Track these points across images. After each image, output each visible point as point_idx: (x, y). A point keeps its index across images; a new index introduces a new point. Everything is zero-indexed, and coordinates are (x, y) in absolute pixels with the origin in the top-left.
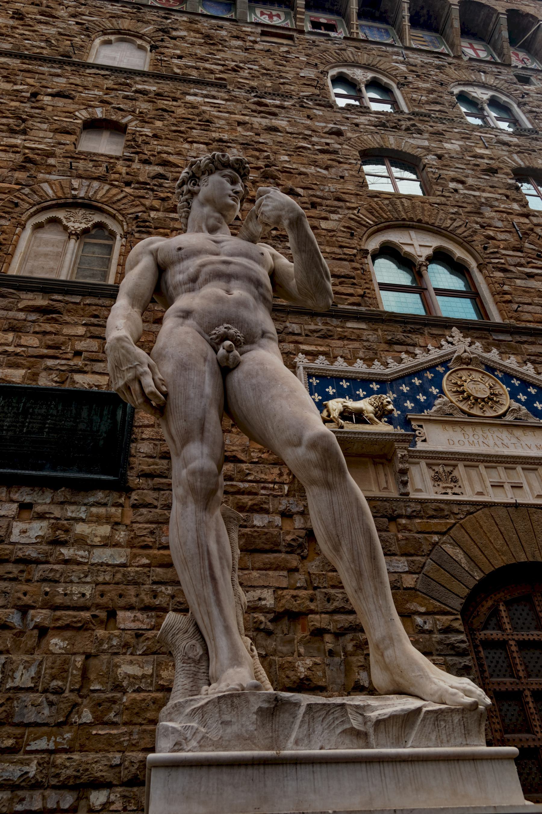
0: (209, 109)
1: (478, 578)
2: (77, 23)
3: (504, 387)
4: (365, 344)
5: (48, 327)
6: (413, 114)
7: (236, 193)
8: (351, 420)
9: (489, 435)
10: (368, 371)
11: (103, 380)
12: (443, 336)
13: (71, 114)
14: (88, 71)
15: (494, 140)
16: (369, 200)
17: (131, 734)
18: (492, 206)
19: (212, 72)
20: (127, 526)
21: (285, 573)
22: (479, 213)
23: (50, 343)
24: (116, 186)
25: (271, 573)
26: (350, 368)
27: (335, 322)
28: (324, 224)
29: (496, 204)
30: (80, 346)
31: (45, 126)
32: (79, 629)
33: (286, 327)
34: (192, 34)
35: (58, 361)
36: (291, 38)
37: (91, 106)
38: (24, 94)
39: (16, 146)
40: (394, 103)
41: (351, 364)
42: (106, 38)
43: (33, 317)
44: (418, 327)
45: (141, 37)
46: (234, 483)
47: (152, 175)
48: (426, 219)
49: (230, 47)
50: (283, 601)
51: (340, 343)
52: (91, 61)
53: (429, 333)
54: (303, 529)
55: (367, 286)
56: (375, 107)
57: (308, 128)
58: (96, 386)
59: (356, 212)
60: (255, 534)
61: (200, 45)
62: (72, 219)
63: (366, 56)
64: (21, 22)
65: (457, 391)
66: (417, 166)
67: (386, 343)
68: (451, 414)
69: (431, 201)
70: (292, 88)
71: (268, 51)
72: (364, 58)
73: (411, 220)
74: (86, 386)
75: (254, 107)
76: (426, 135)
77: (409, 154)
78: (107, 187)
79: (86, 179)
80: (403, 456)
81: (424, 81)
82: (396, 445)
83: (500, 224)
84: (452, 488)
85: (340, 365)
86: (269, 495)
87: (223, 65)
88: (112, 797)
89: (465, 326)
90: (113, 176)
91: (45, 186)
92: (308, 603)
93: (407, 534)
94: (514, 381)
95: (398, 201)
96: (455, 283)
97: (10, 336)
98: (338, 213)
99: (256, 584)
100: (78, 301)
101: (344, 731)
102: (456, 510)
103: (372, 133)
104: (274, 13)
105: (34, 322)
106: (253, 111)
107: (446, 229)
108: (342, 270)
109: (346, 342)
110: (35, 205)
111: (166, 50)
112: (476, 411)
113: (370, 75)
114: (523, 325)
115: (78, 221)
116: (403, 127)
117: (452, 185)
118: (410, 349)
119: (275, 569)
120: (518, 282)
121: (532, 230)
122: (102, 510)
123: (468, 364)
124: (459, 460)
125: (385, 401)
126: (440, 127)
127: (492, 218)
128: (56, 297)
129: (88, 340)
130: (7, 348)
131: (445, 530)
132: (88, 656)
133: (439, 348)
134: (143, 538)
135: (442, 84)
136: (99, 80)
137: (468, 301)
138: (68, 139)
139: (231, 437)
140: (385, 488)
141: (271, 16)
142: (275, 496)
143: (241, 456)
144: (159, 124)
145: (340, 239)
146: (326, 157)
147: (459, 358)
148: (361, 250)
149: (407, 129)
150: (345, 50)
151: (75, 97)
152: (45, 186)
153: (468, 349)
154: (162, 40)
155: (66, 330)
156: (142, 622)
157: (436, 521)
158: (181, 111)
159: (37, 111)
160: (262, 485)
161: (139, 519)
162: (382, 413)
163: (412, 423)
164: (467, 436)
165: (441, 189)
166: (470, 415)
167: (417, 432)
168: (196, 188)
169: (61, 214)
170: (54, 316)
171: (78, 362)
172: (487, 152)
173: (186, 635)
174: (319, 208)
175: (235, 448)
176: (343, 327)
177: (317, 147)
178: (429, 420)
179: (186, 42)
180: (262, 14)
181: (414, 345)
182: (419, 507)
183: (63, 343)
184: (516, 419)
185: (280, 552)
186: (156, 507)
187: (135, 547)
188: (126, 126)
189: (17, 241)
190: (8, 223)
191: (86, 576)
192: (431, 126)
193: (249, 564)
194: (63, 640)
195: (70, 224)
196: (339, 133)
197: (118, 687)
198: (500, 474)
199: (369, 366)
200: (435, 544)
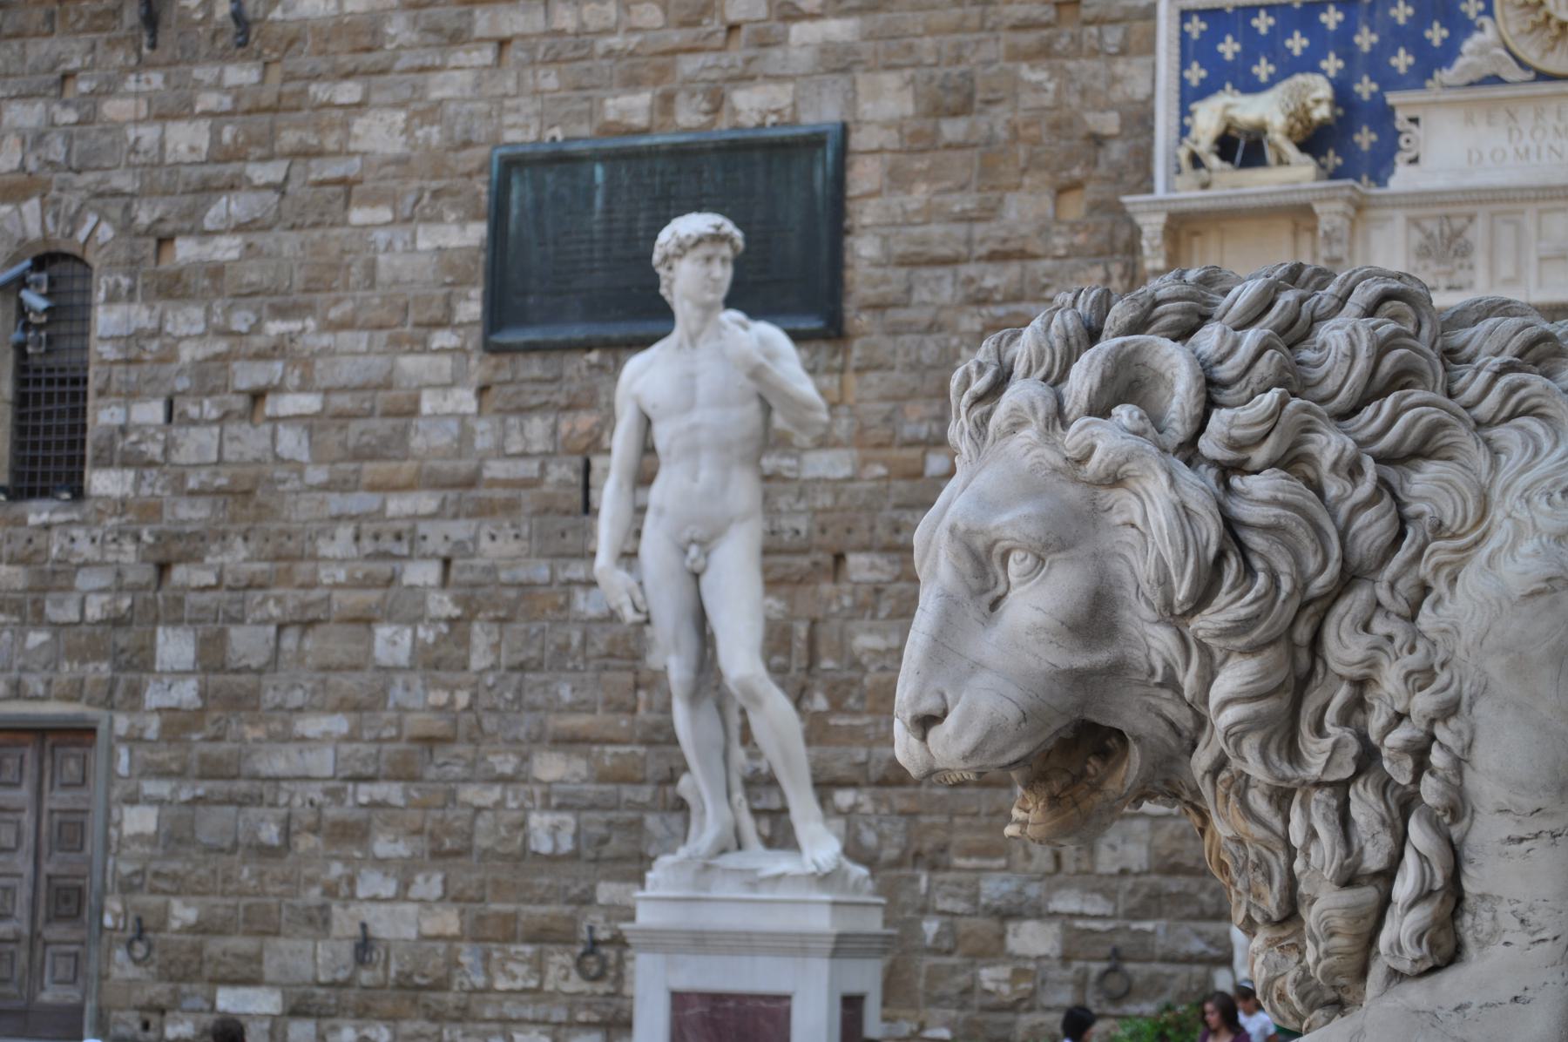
11: (781, 96)
17: (877, 724)
20: (851, 407)
32: (800, 582)
58: (776, 112)
68: (1495, 80)
82: (1317, 208)
88: (861, 799)
124: (1480, 202)
125: (1310, 104)
132: (814, 623)
143: (1034, 246)
156: (882, 571)
164: (1516, 134)
168: (671, 275)
171: (736, 55)
175: (1024, 230)
186: (892, 368)
191: (798, 500)
194: (780, 598)
197: (856, 664)
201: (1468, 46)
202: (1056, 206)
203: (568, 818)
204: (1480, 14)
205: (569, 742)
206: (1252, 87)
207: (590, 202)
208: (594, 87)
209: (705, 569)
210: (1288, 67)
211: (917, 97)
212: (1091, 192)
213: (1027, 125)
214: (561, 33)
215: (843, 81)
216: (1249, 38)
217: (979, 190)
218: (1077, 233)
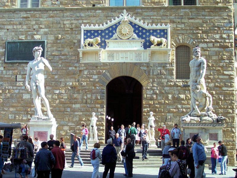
9: (124, 44)
12: (121, 12)
25: (71, 79)
27: (93, 11)
30: (34, 27)
46: (66, 60)
53: (118, 12)
68: (116, 39)
97: (20, 26)
100: (33, 13)
129: (36, 25)
143: (68, 54)
166: (121, 39)
176: (95, 13)
181: (113, 17)
184: (133, 39)
201: (114, 35)
203: (13, 115)
205: (12, 107)
206: (91, 38)
207: (17, 47)
210: (95, 37)
211: (55, 38)
215: (46, 35)
216: (91, 33)
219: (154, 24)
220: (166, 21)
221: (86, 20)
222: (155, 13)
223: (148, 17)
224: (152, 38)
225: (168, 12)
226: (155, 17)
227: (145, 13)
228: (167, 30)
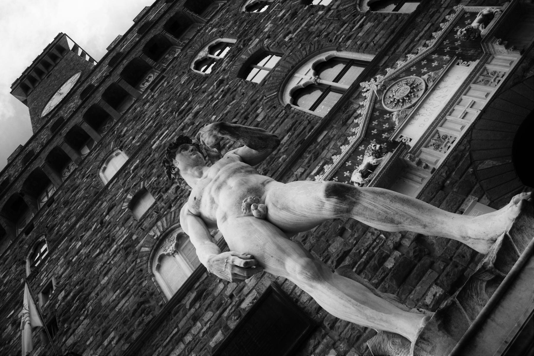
0: (165, 140)
1: (510, 161)
2: (87, 178)
3: (411, 76)
4: (335, 138)
5: (208, 302)
6: (239, 38)
7: (192, 150)
8: (370, 173)
10: (350, 146)
12: (361, 92)
13: (121, 211)
14: (109, 188)
15: (280, 5)
16: (264, 87)
18: (312, 25)
19: (151, 127)
20: (339, 340)
21: (430, 270)
22: (311, 33)
23: (216, 306)
24: (167, 214)
25: (424, 279)
26: (342, 155)
27: (312, 147)
28: (259, 119)
29: (312, 22)
31: (118, 228)
33: (296, 175)
34: (128, 125)
35: (228, 310)
36: (163, 77)
37: (124, 199)
38: (98, 227)
39: (116, 249)
40: (228, 44)
41: (340, 153)
42: (102, 168)
43: (197, 305)
44: (346, 103)
45: (113, 152)
46: (359, 263)
47: (174, 191)
48: (294, 63)
49: (147, 110)
50: (445, 283)
51: (325, 152)
52: (106, 183)
54: (412, 242)
55: (306, 116)
56: (222, 56)
57: (208, 96)
58: (254, 299)
59: (265, 98)
60: (395, 271)
61: (135, 124)
62: (167, 248)
63: (196, 45)
64: (70, 204)
65: (396, 104)
66: (266, 51)
67: (343, 126)
69: (287, 55)
70: (185, 91)
71: (161, 92)
72: (197, 46)
73: (289, 71)
74: (250, 305)
75: (180, 117)
76: (254, 38)
77: (256, 52)
78: (164, 219)
79: (153, 226)
80: (410, 158)
81: (228, 23)
83: (324, 26)
84: (448, 142)
85: (336, 159)
86: (379, 249)
87: (151, 119)
89: (364, 77)
90: (161, 212)
91: (144, 249)
92: (456, 270)
93: (457, 185)
94: (412, 69)
95: (275, 72)
96: (339, 68)
97: (199, 324)
98: (259, 108)
99: (424, 292)
101: (487, 287)
102: (462, 148)
103: (233, 65)
104: (147, 78)
105: (200, 307)
106: (181, 119)
107: (306, 56)
108: (288, 125)
109: (327, 148)
110: (147, 262)
111: (126, 143)
112: (414, 101)
113: (207, 49)
114: (385, 45)
115: (170, 246)
116: (242, 47)
117: (287, 39)
118: (355, 115)
119: (424, 274)
120: (360, 34)
121: (338, 11)
122: (321, 347)
123: (385, 89)
124: (435, 127)
125: (373, 148)
126: (255, 28)
127: (318, 28)
128: (196, 286)
130: (203, 331)
131: (469, 162)
133: (366, 99)
134: (352, 336)
135: (236, 15)
136: (117, 186)
137: (352, 67)
138: (131, 222)
139: (333, 247)
140: (422, 180)
141: (147, 81)
142: (383, 245)
143: (347, 248)
144: (155, 171)
145: (272, 115)
146: (228, 95)
147: (378, 91)
148: (285, 108)
149: (244, 45)
150: (187, 54)
151: (115, 203)
152: (144, 249)
153: (376, 83)
154: (121, 142)
155: (216, 293)
157: (461, 163)
158: (157, 155)
159: (109, 226)
160: (371, 248)
161: (340, 331)
162: (378, 154)
163: (396, 140)
165: (284, 46)
166: (414, 105)
167: (403, 141)
168: (176, 170)
169: (161, 252)
170: (204, 294)
172: (283, 11)
173: (385, 341)
174: (249, 116)
175: (340, 249)
176: (318, 144)
177: (220, 98)
178: (401, 129)
179: (130, 130)
180: (143, 84)
181: (355, 111)
182: (446, 168)
183: (221, 300)
185: (416, 265)
187: (354, 344)
188: (144, 187)
189: (158, 284)
190: (146, 282)
192: (251, 32)
193: (410, 287)
195: (168, 251)
196: (221, 82)
198: (459, 110)
199: (348, 144)
200: (474, 173)
202: (343, 238)
204: (389, 115)
208: (205, 345)
209: (266, 209)
212: (347, 227)
213: (318, 234)
214: (190, 342)
217: (320, 257)
218: (354, 235)
219: (434, 34)
220: (448, 11)
221: (315, 168)
222: (414, 31)
223: (412, 45)
224: (461, 32)
225: (430, 10)
226: (421, 34)
227: (397, 51)
228: (466, 13)
